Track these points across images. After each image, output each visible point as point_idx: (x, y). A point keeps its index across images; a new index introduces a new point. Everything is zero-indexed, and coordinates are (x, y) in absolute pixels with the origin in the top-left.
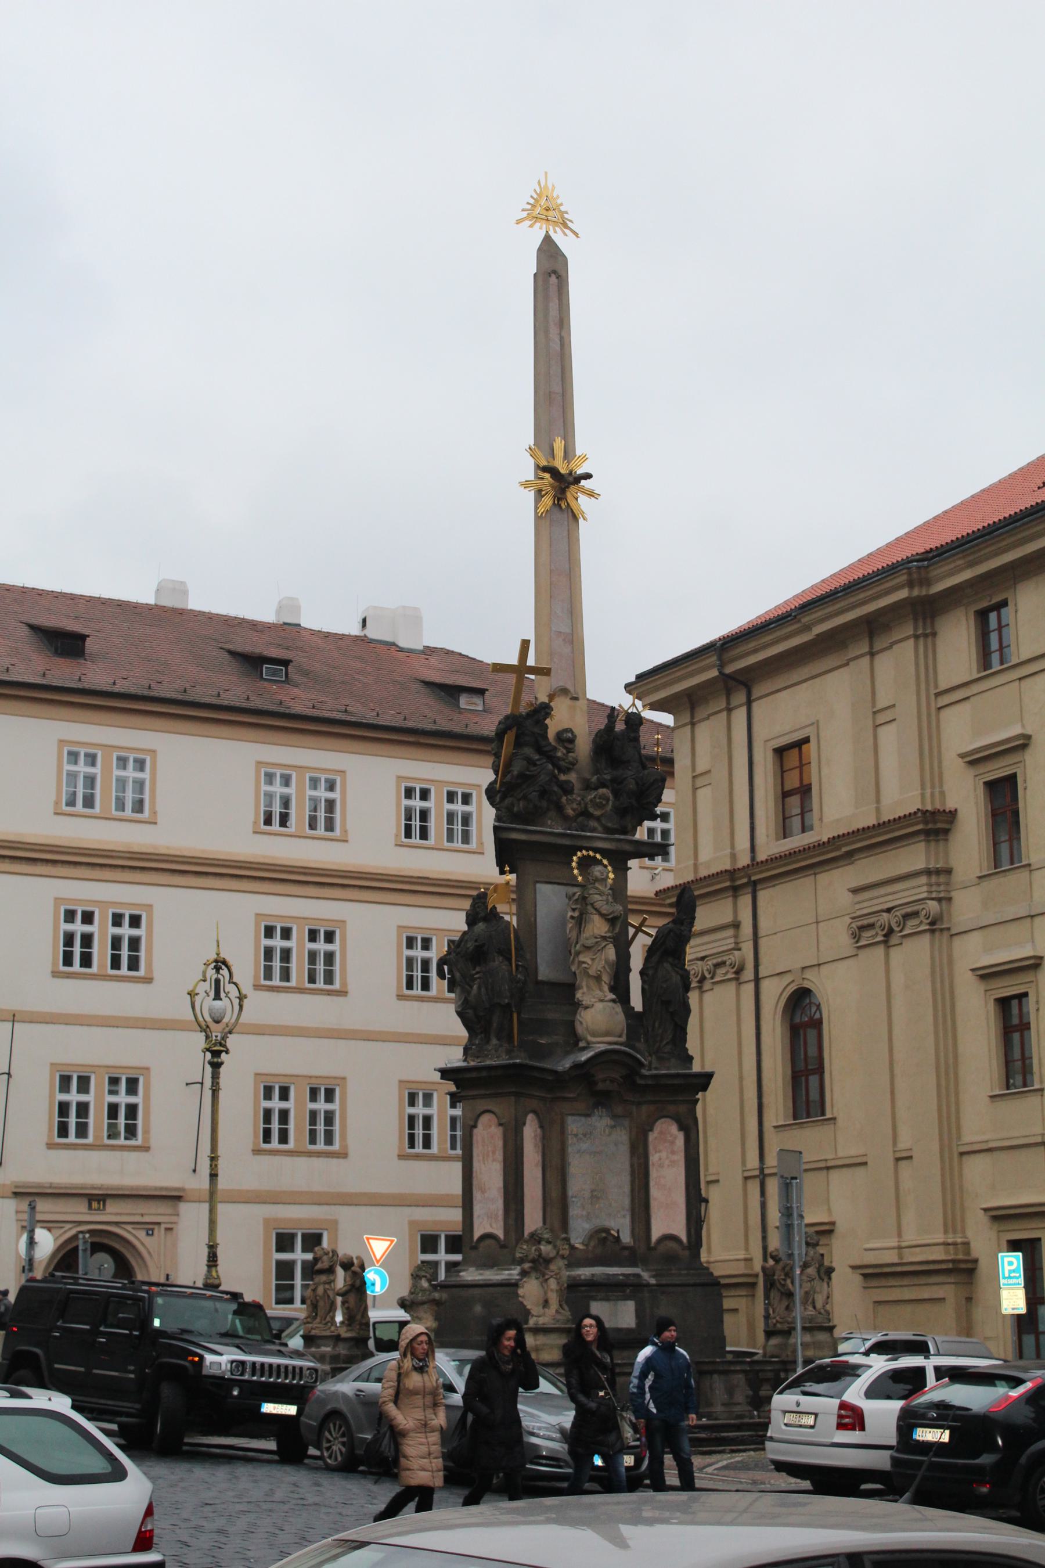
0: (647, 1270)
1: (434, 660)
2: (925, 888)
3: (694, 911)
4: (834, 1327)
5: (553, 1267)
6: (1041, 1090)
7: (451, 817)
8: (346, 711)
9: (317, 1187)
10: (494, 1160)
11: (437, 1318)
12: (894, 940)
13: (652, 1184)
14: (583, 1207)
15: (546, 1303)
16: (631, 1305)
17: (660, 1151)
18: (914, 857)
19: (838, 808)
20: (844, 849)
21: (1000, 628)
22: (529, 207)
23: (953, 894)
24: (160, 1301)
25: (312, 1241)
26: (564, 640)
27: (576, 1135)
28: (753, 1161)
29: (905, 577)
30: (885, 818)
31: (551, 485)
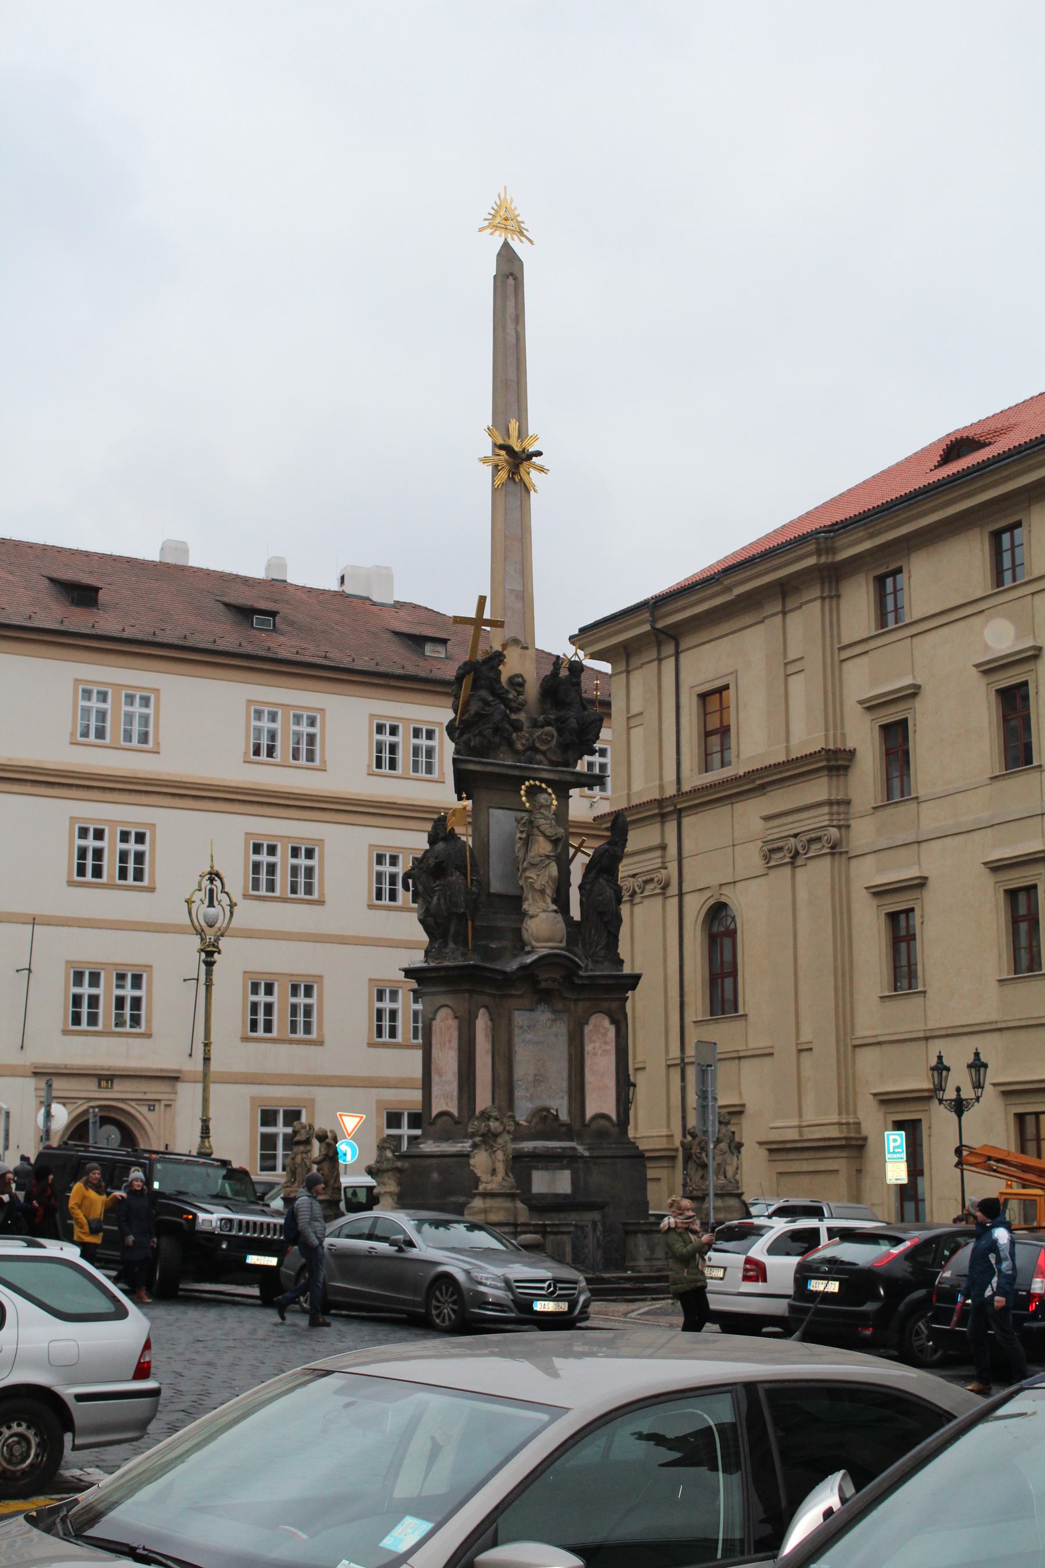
0: (582, 1144)
1: (402, 613)
2: (827, 817)
3: (626, 834)
4: (742, 1194)
5: (500, 1140)
6: (924, 992)
7: (416, 750)
8: (326, 657)
9: (297, 1071)
10: (450, 1048)
11: (399, 1184)
12: (800, 861)
13: (587, 1070)
14: (527, 1089)
15: (494, 1172)
16: (567, 1174)
17: (594, 1042)
18: (818, 790)
19: (754, 745)
20: (758, 782)
21: (895, 591)
22: (490, 217)
23: (851, 822)
24: (159, 1166)
25: (292, 1116)
27: (521, 1027)
28: (675, 1052)
29: (813, 547)
30: (794, 755)
31: (506, 461)
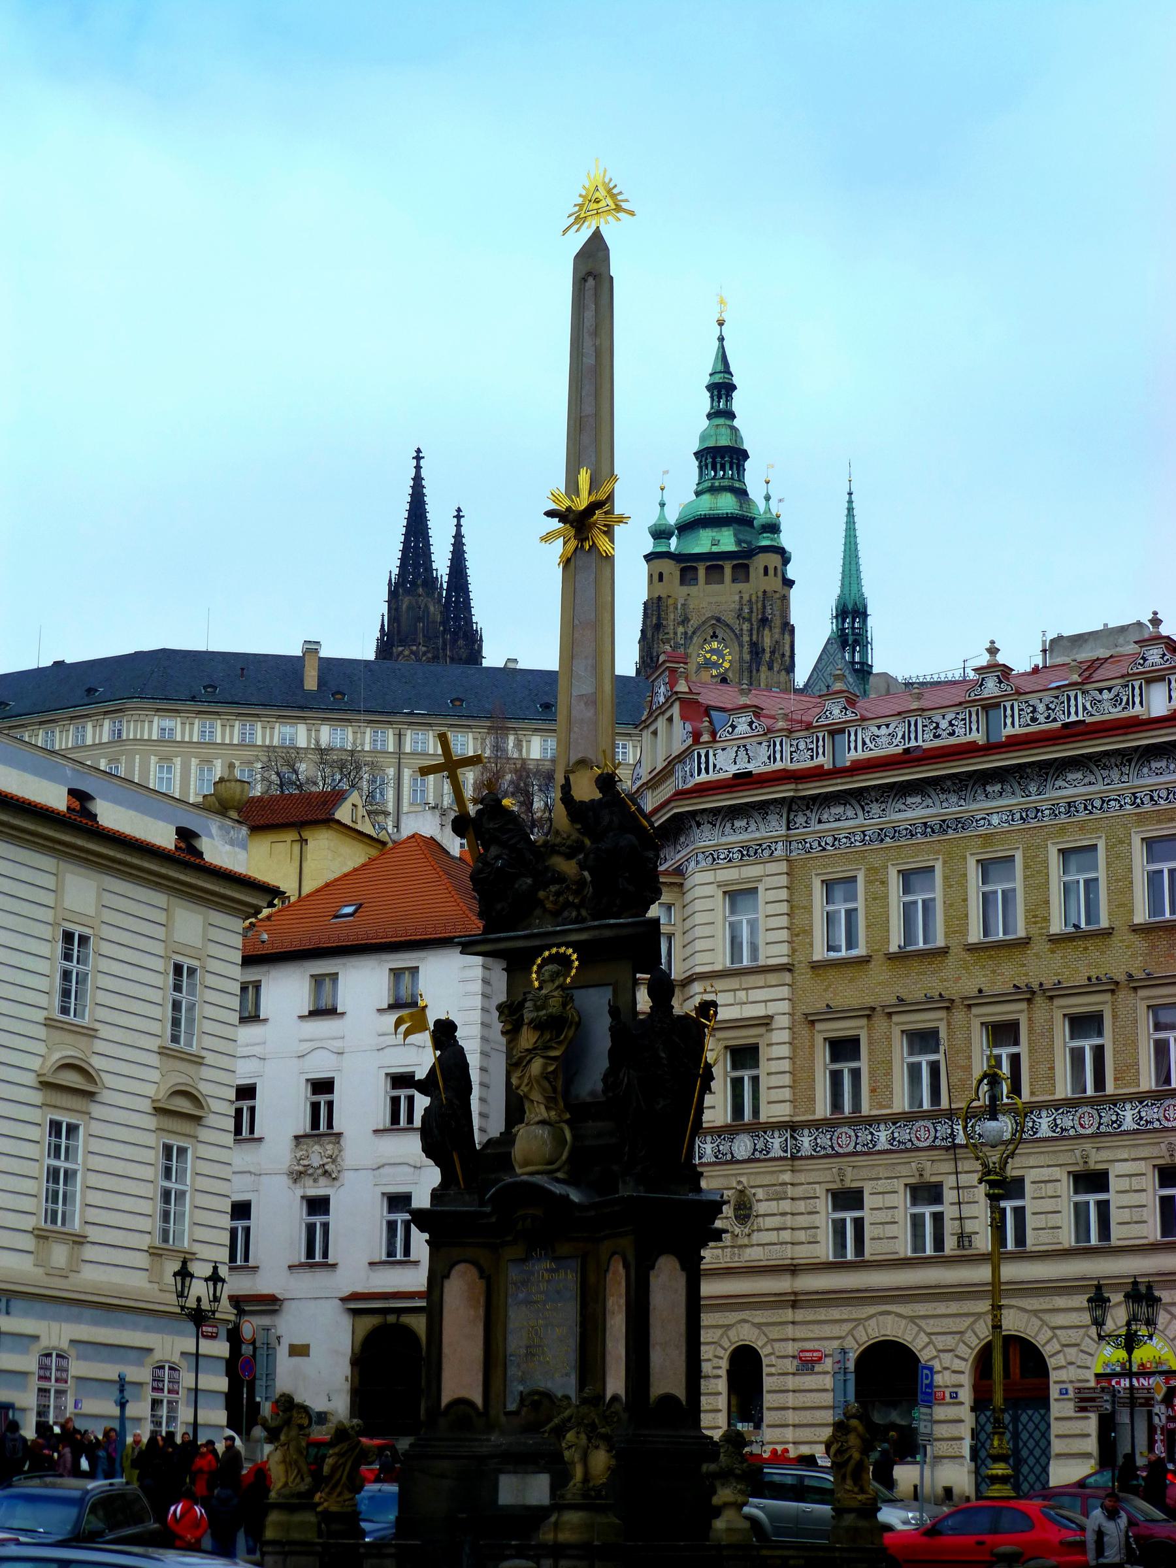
14: (519, 1366)
26: (586, 704)
